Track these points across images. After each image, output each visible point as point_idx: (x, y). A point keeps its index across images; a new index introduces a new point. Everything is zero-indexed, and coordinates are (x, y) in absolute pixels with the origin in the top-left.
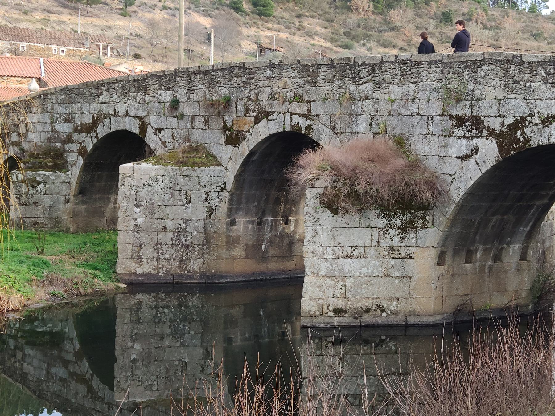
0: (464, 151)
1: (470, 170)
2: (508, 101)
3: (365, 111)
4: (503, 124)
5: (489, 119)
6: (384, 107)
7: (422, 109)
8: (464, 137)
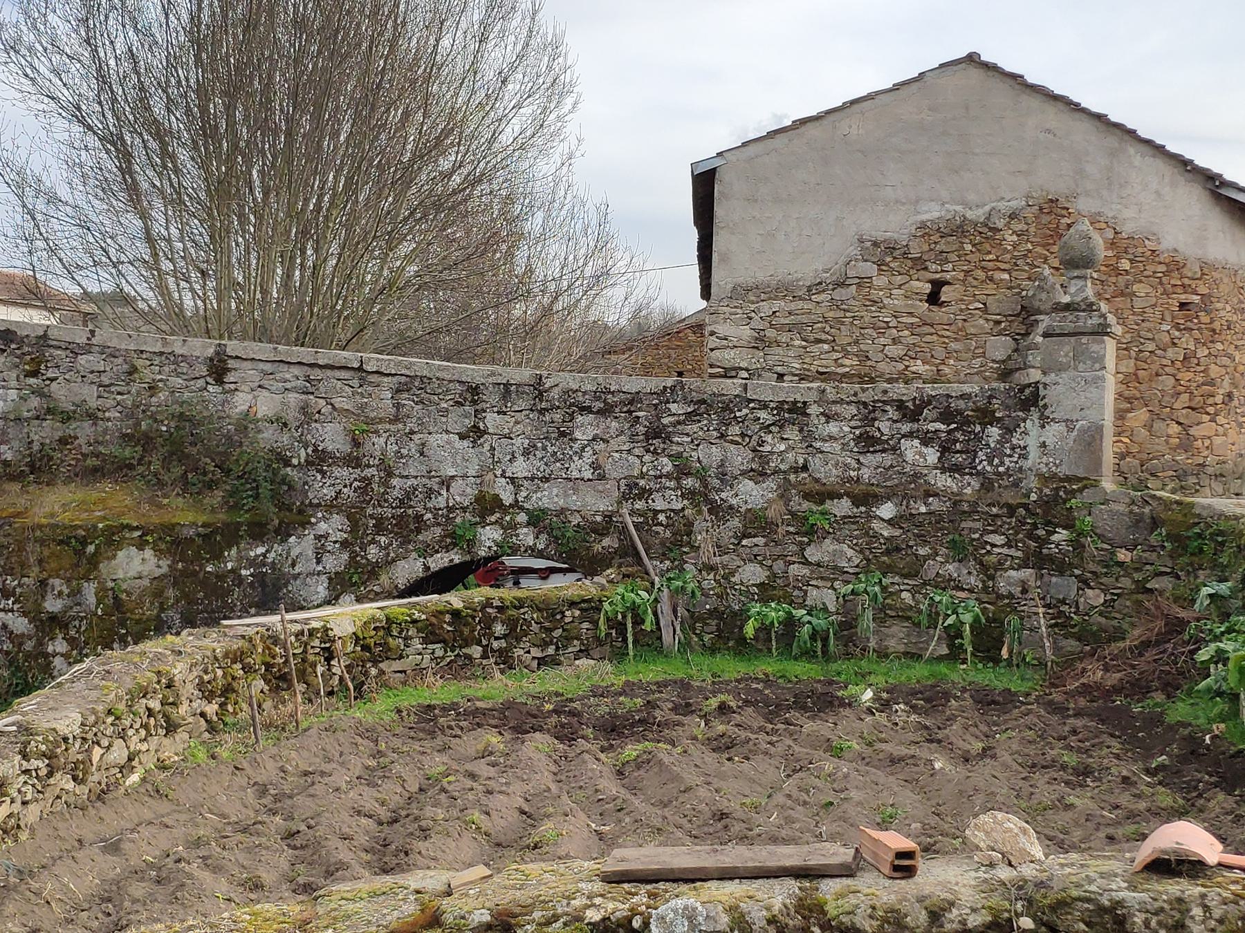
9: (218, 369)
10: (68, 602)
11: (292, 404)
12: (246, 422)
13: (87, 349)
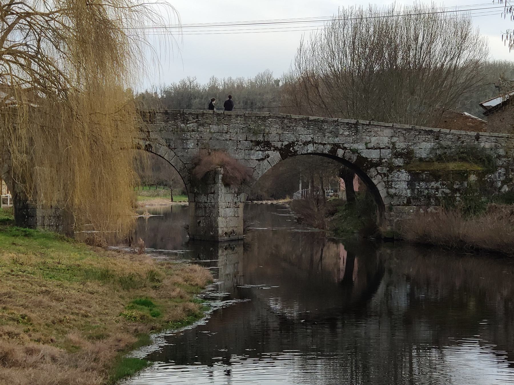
0: (260, 157)
1: (264, 165)
2: (284, 135)
3: (192, 137)
4: (282, 145)
5: (274, 142)
6: (206, 136)
7: (233, 137)
8: (260, 150)
9: (477, 138)
10: (460, 186)
11: (493, 145)
12: (484, 149)
13: (449, 134)
